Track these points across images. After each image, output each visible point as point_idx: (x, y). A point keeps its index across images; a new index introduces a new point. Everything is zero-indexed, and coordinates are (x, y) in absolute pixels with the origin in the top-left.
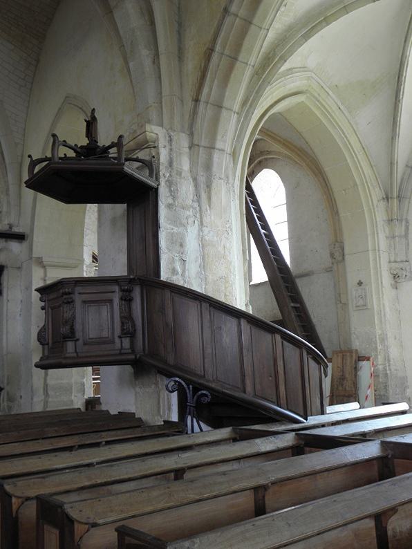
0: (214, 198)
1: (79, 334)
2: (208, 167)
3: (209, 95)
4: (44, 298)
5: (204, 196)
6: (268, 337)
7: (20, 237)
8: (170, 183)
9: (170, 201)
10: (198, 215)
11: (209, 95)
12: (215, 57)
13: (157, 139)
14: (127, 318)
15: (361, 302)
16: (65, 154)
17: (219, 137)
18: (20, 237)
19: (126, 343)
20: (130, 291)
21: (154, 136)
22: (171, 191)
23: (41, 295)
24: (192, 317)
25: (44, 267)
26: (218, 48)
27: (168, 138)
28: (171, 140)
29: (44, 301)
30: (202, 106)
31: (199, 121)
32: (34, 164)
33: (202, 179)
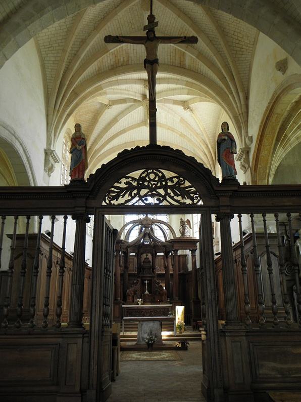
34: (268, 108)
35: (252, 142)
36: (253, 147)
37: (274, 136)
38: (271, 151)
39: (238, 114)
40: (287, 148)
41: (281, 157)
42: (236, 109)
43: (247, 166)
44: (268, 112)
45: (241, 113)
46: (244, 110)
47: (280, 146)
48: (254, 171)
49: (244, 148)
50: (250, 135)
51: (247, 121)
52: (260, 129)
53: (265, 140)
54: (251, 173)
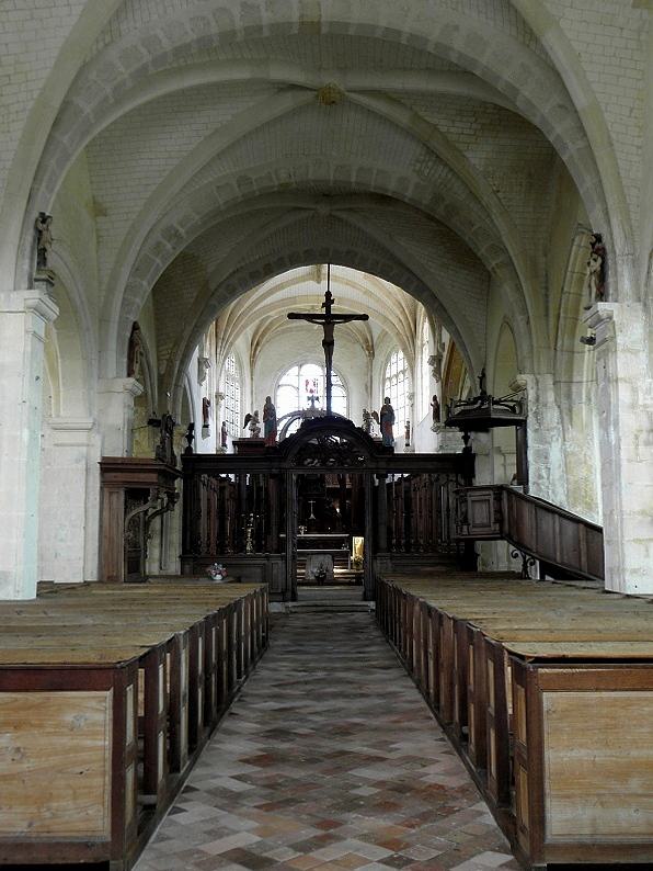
0: (574, 417)
2: (569, 396)
3: (562, 345)
5: (566, 418)
8: (536, 414)
11: (562, 345)
12: (562, 321)
13: (526, 384)
14: (499, 511)
17: (575, 373)
20: (501, 494)
24: (527, 510)
25: (503, 454)
26: (562, 315)
28: (537, 382)
30: (558, 353)
33: (565, 406)
35: (444, 350)
36: (445, 354)
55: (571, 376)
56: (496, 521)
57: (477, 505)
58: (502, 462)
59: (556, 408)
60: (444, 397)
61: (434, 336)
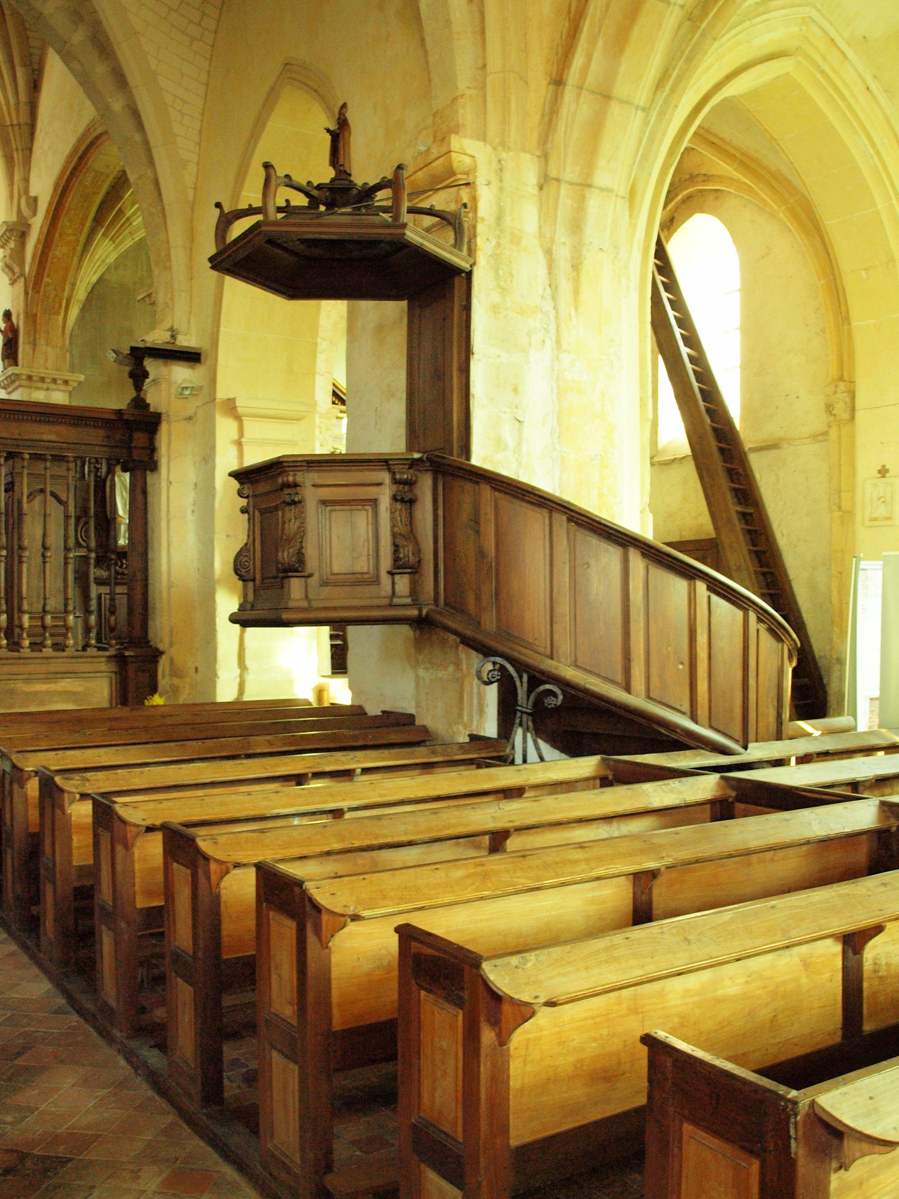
1: (312, 564)
2: (577, 226)
4: (246, 492)
5: (565, 287)
6: (679, 586)
7: (192, 357)
9: (496, 297)
10: (552, 328)
13: (473, 169)
15: (881, 511)
16: (287, 201)
17: (601, 162)
18: (192, 357)
19: (403, 583)
20: (410, 483)
21: (467, 160)
22: (497, 277)
23: (241, 483)
25: (238, 418)
27: (495, 165)
29: (247, 497)
31: (561, 126)
32: (226, 220)
33: (563, 253)
34: (75, 149)
35: (35, 213)
36: (38, 223)
37: (85, 217)
38: (79, 249)
39: (8, 123)
40: (120, 243)
41: (104, 261)
42: (4, 108)
43: (17, 270)
44: (76, 159)
45: (15, 122)
46: (24, 118)
47: (103, 235)
48: (33, 288)
49: (14, 223)
50: (33, 193)
51: (29, 150)
52: (55, 190)
53: (64, 221)
54: (26, 293)
55: (589, 166)
56: (399, 566)
57: (339, 517)
58: (235, 435)
59: (540, 254)
60: (31, 318)
61: (11, 184)
